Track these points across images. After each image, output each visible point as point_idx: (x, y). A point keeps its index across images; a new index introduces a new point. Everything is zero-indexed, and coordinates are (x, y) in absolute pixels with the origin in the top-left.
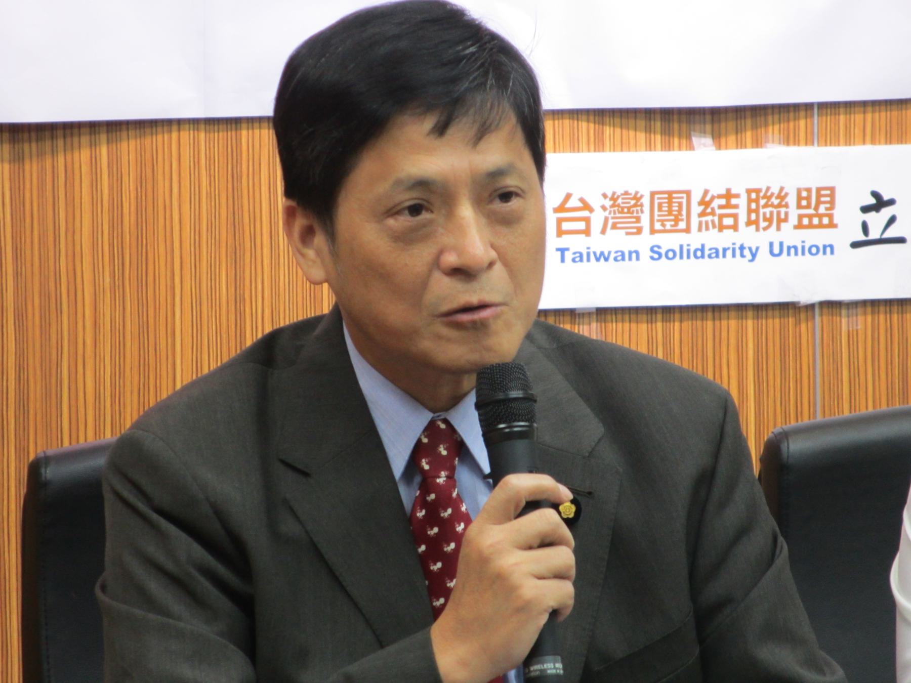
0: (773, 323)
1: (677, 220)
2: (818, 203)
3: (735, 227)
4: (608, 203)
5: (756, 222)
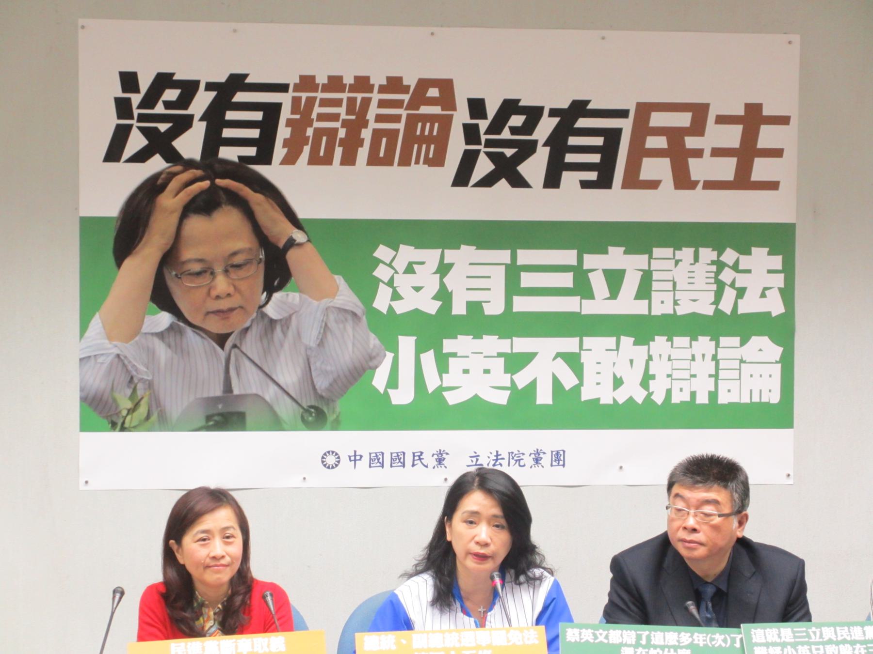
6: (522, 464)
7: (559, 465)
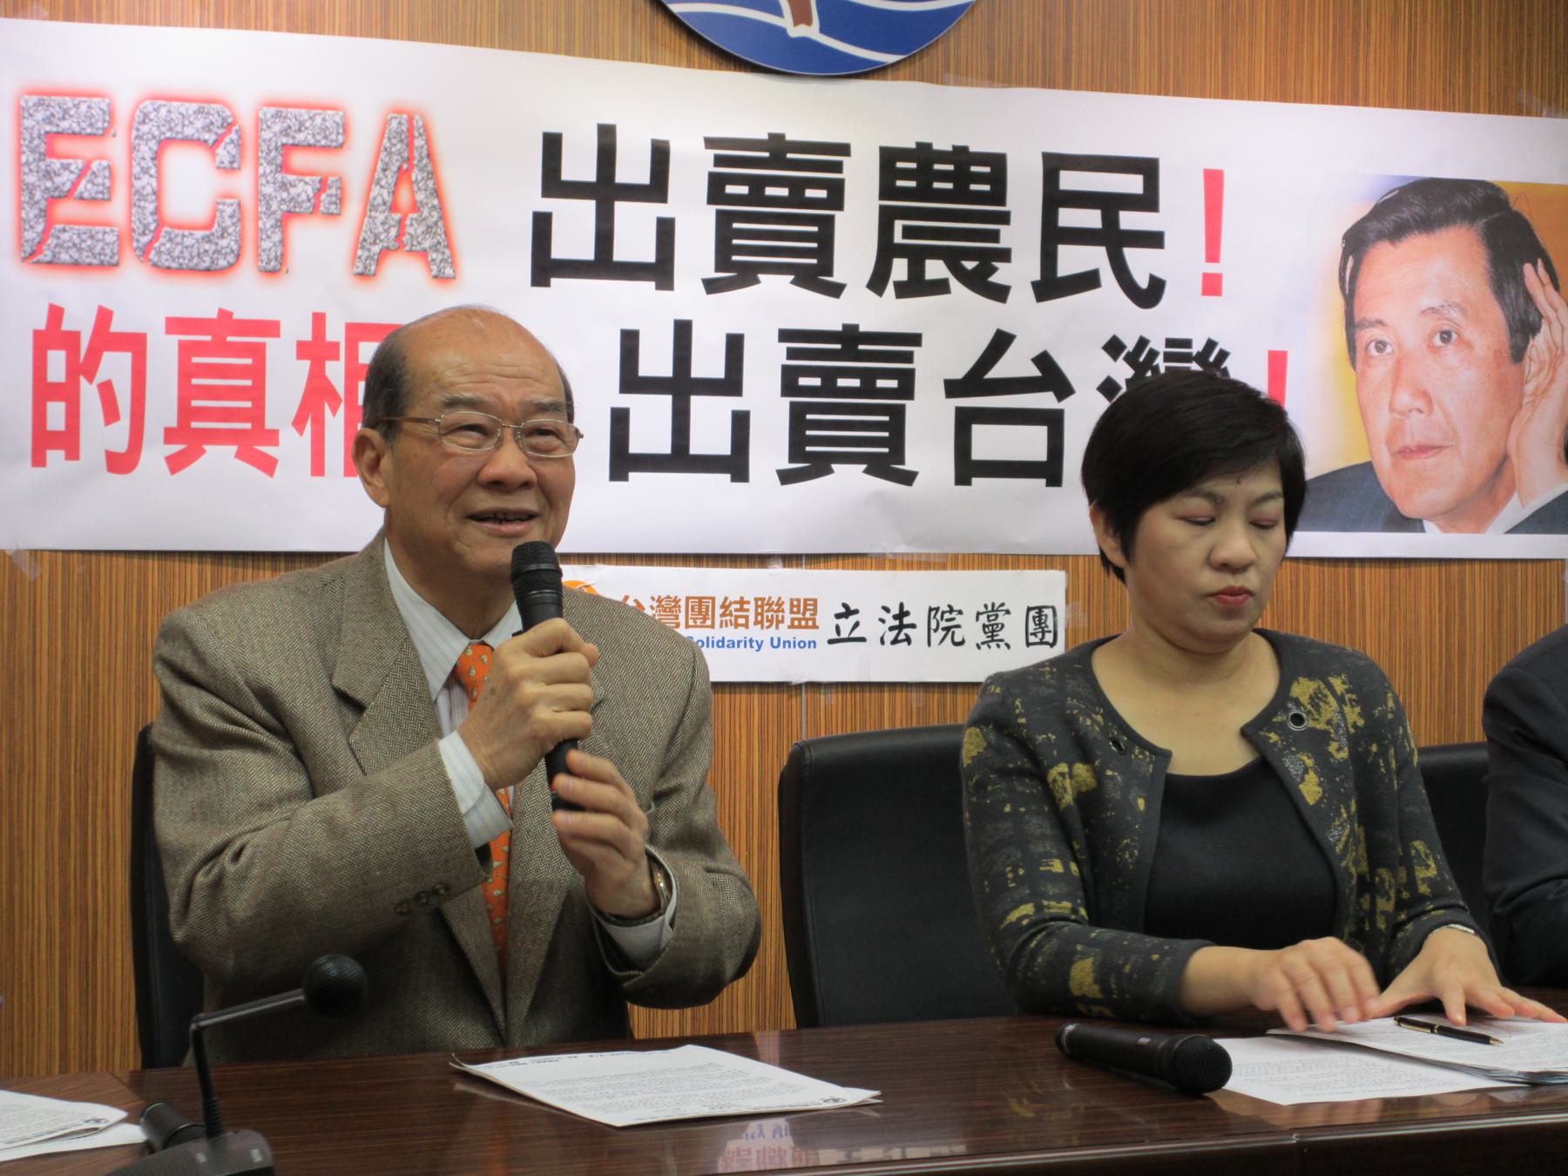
0: (773, 698)
1: (705, 619)
2: (806, 610)
3: (746, 626)
4: (655, 604)
5: (761, 623)
6: (958, 639)
7: (1042, 643)
